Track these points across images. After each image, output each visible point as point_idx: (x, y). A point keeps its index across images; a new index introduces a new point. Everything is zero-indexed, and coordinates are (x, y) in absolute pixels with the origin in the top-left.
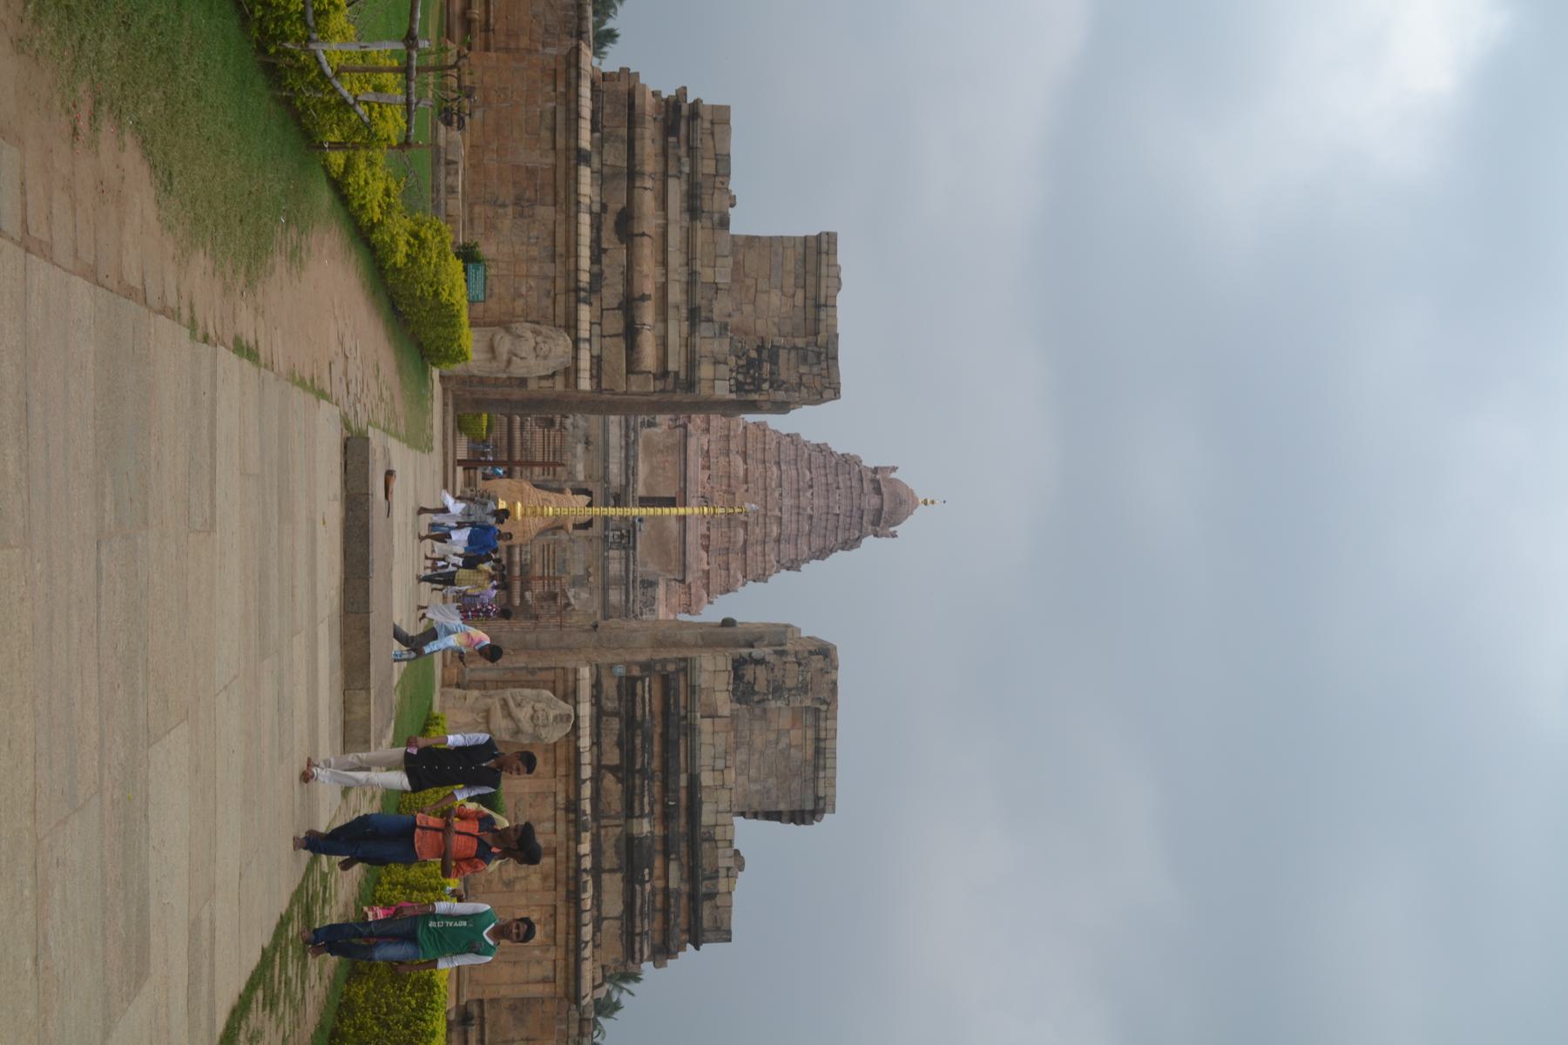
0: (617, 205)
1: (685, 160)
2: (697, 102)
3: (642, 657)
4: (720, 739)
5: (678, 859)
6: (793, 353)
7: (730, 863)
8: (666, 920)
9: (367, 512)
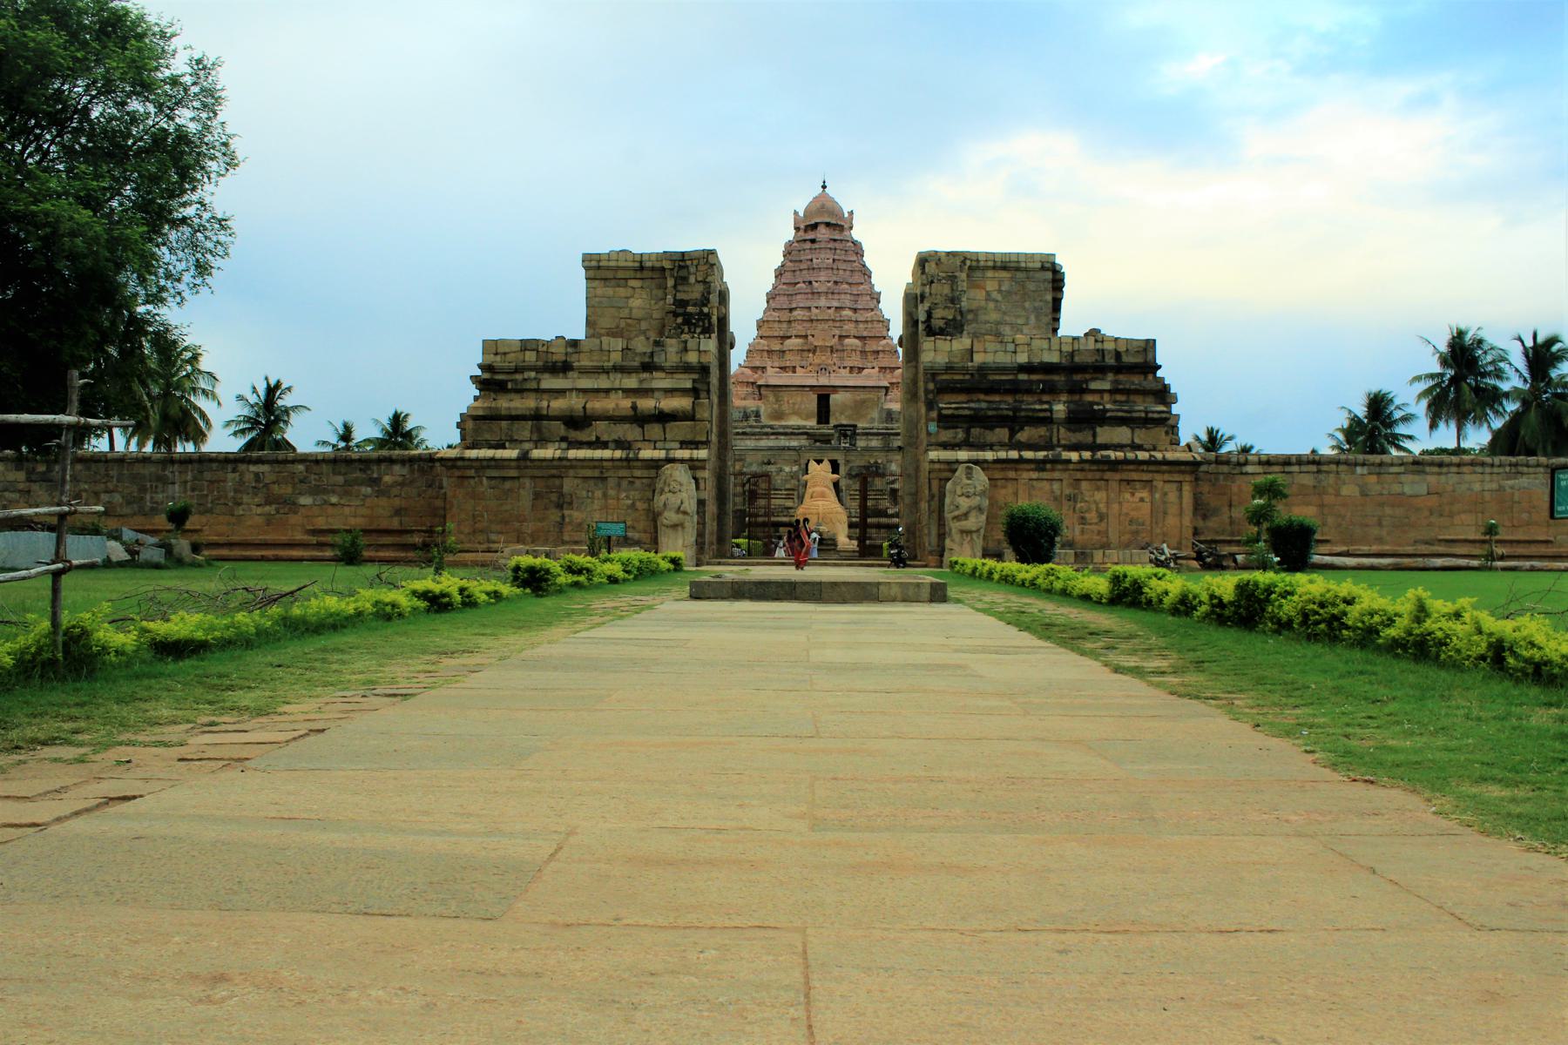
0: (559, 428)
1: (526, 375)
2: (480, 366)
3: (923, 410)
4: (991, 347)
5: (1086, 381)
7: (1091, 339)
8: (1137, 392)
9: (745, 583)
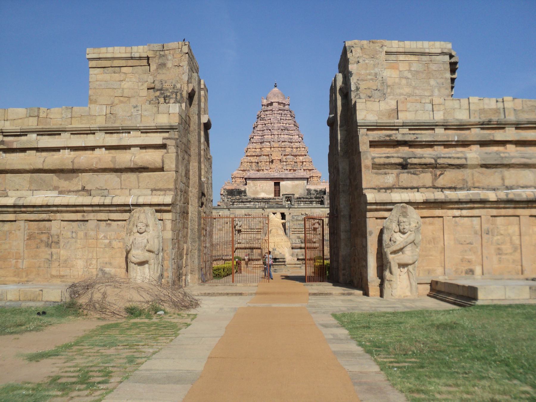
6: (160, 71)
